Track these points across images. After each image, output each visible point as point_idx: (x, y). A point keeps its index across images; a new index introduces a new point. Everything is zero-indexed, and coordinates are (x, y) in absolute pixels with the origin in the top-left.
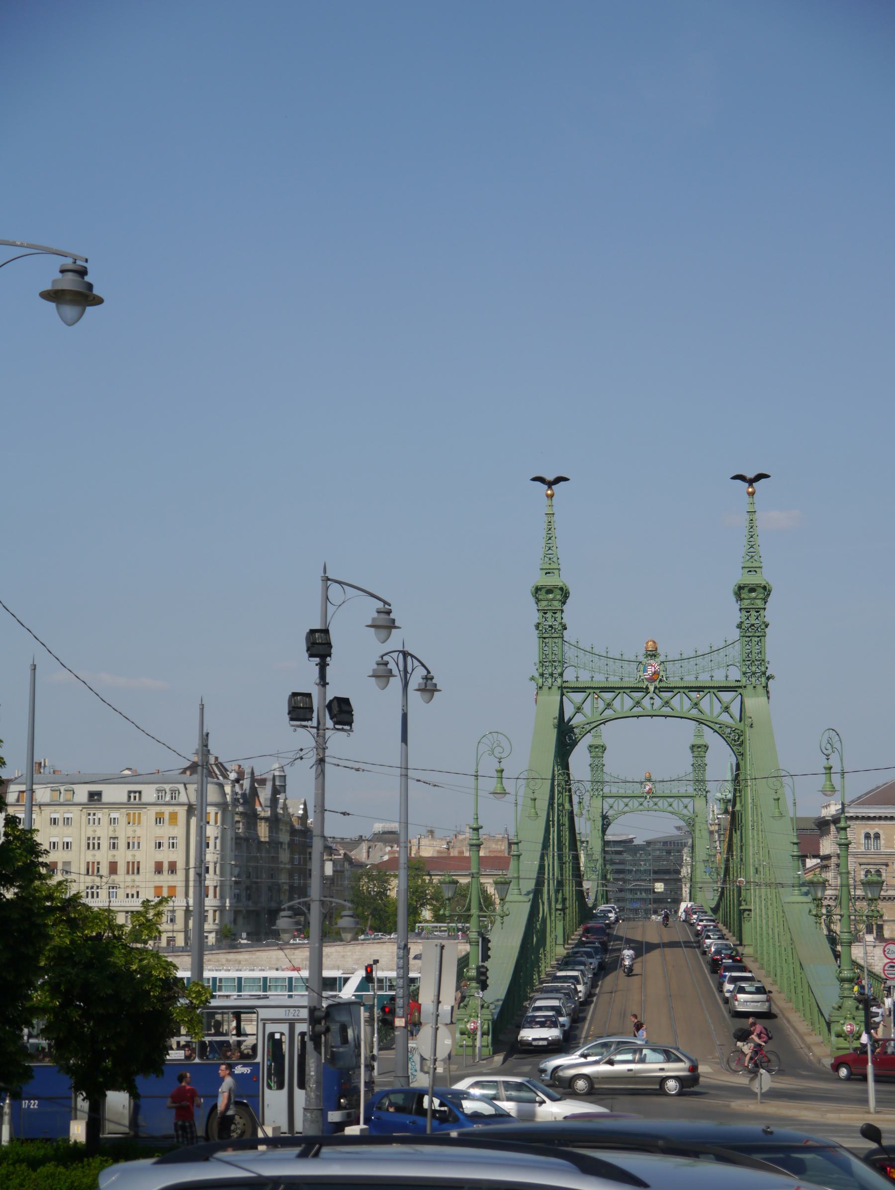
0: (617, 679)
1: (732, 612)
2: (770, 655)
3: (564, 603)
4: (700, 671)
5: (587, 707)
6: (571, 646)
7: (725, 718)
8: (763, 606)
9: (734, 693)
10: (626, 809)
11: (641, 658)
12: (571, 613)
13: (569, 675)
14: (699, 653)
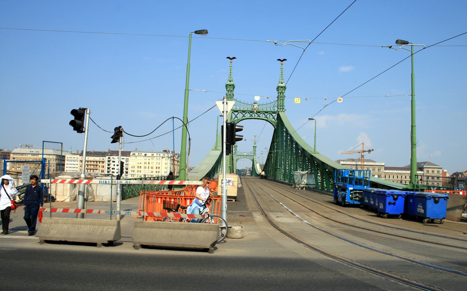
0: (246, 109)
1: (276, 94)
2: (285, 104)
5: (238, 116)
8: (284, 92)
9: (275, 114)
11: (253, 104)
14: (267, 103)
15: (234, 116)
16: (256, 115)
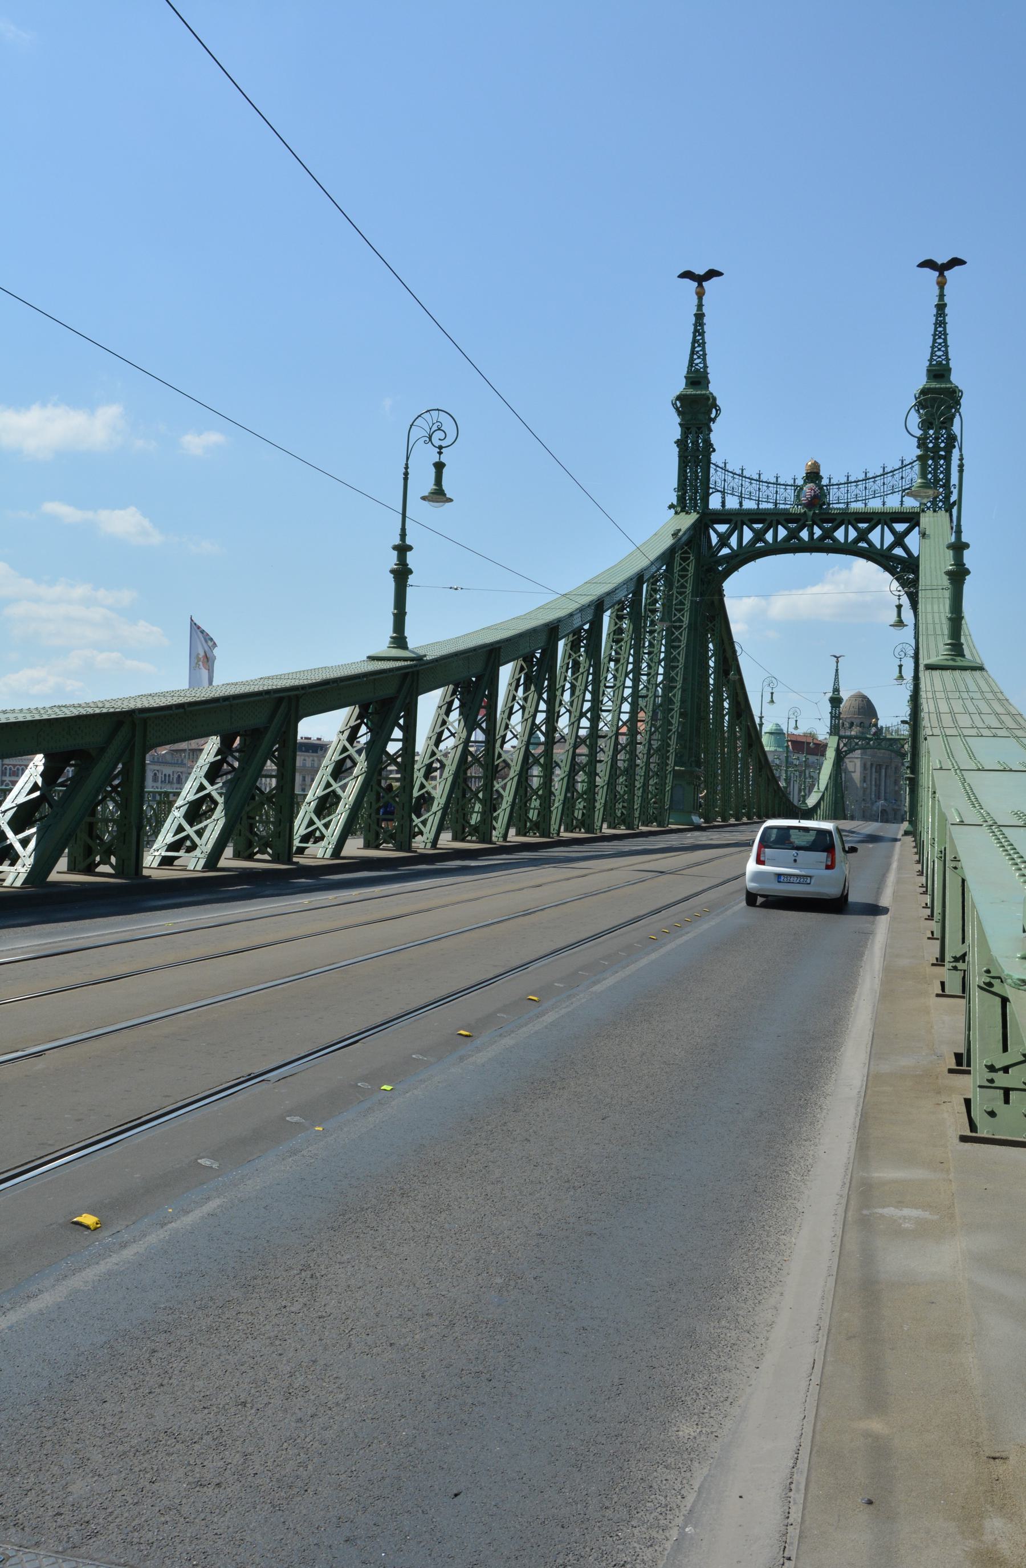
3: (714, 420)
4: (871, 497)
5: (733, 541)
6: (718, 469)
7: (899, 551)
10: (856, 747)
12: (719, 433)
13: (715, 502)
15: (714, 539)
16: (818, 532)
